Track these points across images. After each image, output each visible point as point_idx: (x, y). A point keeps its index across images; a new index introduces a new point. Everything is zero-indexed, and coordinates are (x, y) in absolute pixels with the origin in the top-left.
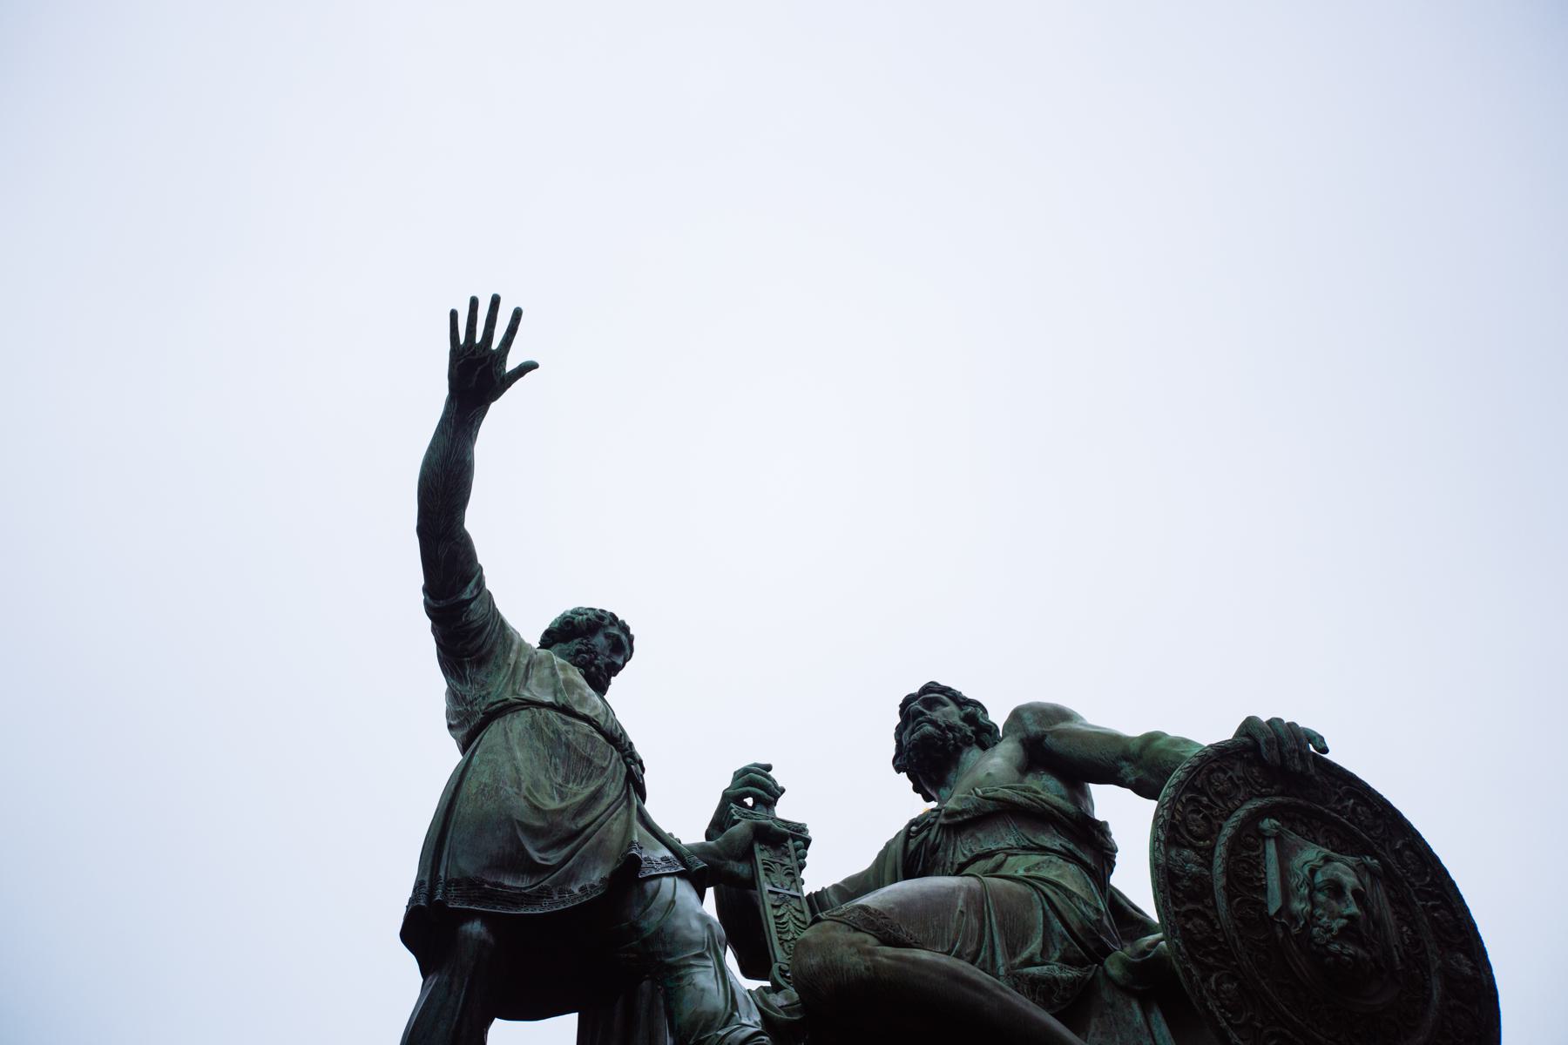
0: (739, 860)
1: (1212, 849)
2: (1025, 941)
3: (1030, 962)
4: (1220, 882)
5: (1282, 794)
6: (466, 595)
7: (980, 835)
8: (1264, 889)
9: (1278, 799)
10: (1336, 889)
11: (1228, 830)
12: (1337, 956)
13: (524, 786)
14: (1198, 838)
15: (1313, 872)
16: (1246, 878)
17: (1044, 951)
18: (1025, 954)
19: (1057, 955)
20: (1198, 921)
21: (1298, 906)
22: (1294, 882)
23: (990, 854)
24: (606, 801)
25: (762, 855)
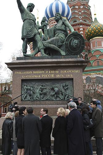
16: (70, 43)
21: (73, 44)
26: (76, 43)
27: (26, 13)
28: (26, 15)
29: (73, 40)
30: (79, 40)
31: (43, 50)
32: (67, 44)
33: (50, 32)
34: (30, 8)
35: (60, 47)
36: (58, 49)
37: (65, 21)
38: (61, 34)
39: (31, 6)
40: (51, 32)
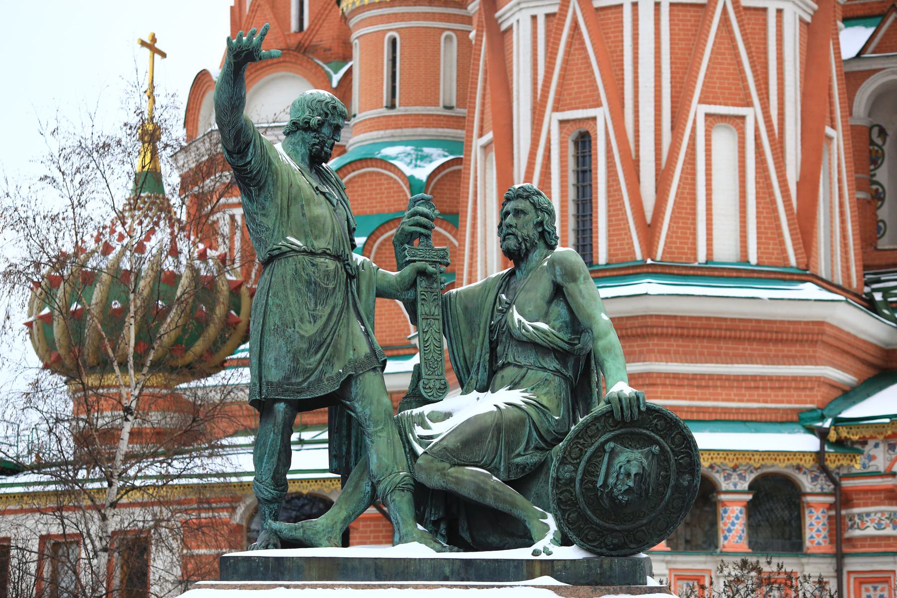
0: (408, 290)
1: (579, 464)
2: (518, 445)
3: (519, 455)
4: (579, 477)
5: (621, 428)
6: (248, 160)
7: (520, 349)
8: (598, 476)
9: (617, 432)
10: (628, 475)
11: (588, 454)
12: (620, 501)
13: (296, 325)
14: (573, 459)
15: (620, 467)
16: (590, 472)
17: (526, 450)
18: (517, 452)
19: (533, 446)
20: (566, 494)
21: (611, 481)
22: (613, 470)
23: (520, 367)
24: (337, 310)
25: (422, 284)
26: (634, 471)
27: (280, 197)
28: (285, 212)
29: (613, 454)
30: (656, 449)
31: (407, 496)
32: (572, 480)
33: (463, 326)
34: (309, 137)
35: (522, 481)
36: (513, 505)
37: (572, 275)
38: (542, 374)
39: (321, 124)
40: (470, 323)
